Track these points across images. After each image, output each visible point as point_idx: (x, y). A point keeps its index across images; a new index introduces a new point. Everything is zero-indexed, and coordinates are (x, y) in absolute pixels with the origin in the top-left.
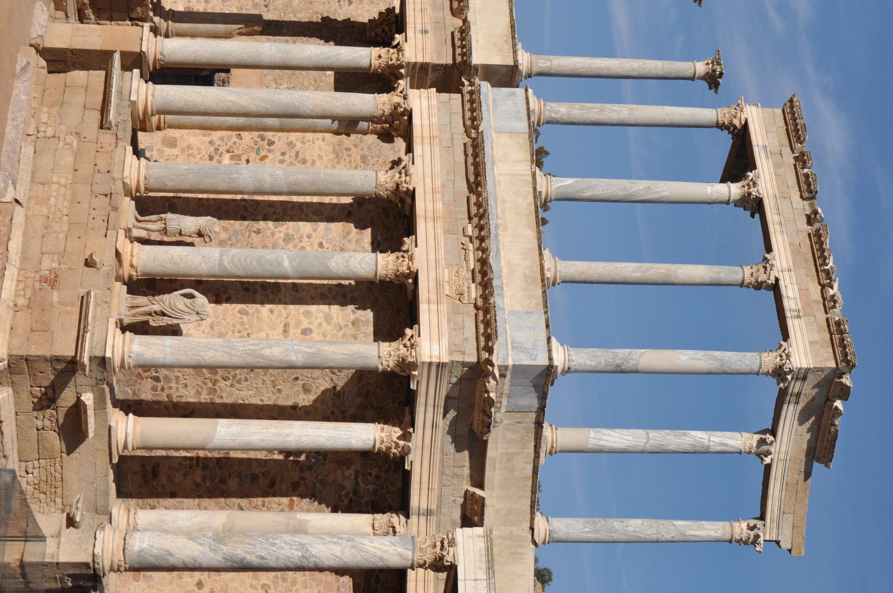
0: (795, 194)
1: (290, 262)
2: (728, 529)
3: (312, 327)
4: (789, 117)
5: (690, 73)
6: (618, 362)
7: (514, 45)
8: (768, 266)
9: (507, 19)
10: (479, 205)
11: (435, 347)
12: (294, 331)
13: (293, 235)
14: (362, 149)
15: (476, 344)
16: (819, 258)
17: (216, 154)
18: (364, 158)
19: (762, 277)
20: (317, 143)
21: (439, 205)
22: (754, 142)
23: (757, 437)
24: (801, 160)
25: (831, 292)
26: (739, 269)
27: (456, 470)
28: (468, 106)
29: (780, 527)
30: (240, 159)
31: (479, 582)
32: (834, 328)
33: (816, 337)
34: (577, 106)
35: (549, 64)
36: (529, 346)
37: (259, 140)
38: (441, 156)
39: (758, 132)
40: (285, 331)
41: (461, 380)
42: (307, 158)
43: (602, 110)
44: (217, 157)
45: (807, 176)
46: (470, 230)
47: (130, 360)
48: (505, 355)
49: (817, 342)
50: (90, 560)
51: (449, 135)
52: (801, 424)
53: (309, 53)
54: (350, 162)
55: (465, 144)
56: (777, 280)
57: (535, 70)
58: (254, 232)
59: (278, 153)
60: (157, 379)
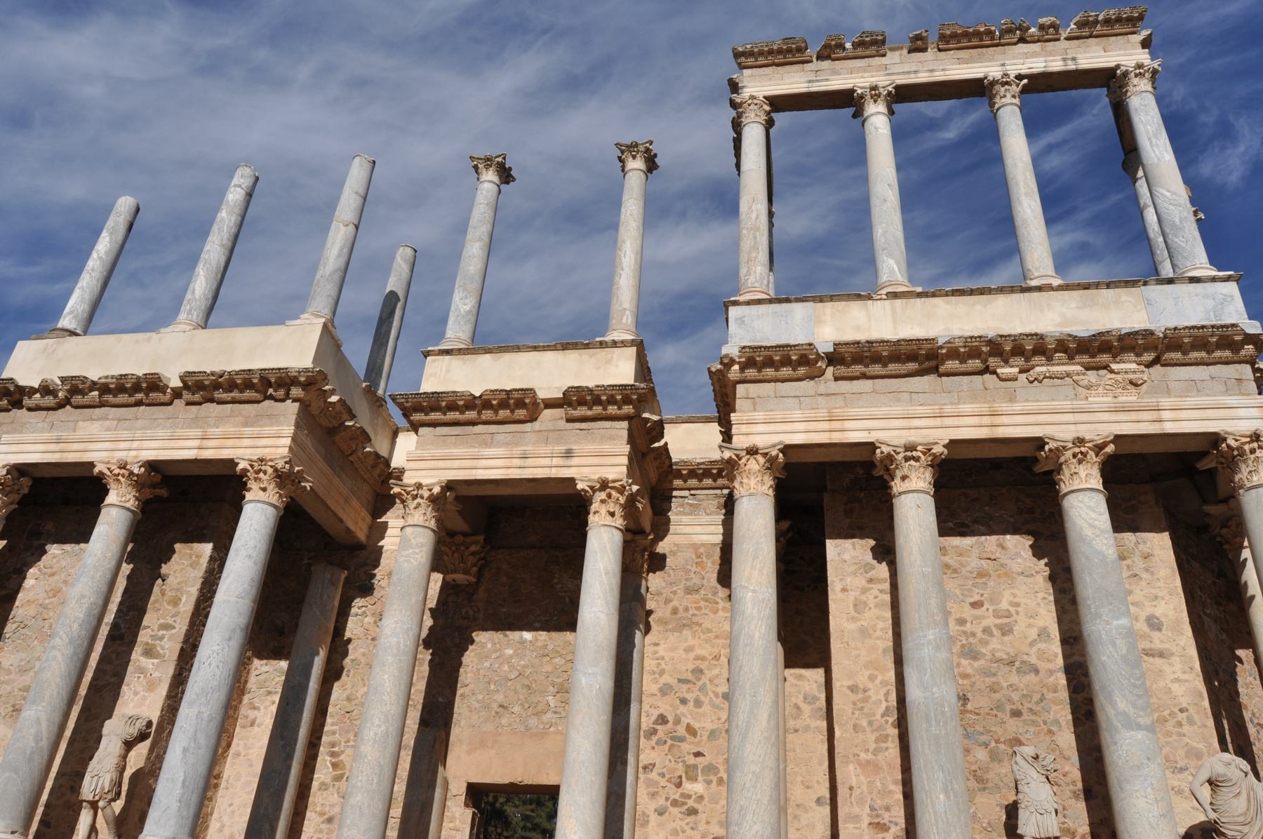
3: (1143, 615)
4: (761, 61)
7: (602, 345)
9: (549, 356)
10: (974, 353)
11: (1242, 412)
12: (1158, 641)
13: (963, 646)
14: (674, 593)
16: (981, 40)
17: (684, 804)
18: (690, 591)
20: (661, 653)
21: (966, 408)
30: (695, 767)
32: (1086, 31)
35: (628, 312)
37: (655, 738)
40: (1161, 654)
42: (691, 667)
44: (691, 803)
45: (856, 45)
51: (820, 398)
53: (603, 616)
54: (698, 609)
55: (836, 379)
58: (964, 705)
59: (682, 709)
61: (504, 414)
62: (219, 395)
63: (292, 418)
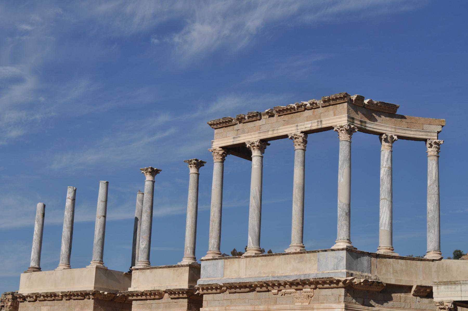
0: (258, 123)
2: (432, 158)
4: (219, 126)
5: (195, 176)
6: (344, 214)
7: (179, 266)
8: (295, 137)
10: (262, 286)
15: (335, 289)
16: (291, 111)
19: (301, 140)
22: (231, 143)
23: (383, 143)
24: (241, 120)
25: (308, 105)
26: (296, 152)
27: (402, 300)
28: (210, 291)
29: (431, 131)
31: (462, 289)
33: (332, 112)
34: (211, 234)
35: (189, 248)
36: (336, 260)
38: (235, 306)
39: (226, 141)
41: (354, 297)
43: (213, 221)
45: (249, 117)
46: (275, 291)
48: (341, 274)
49: (334, 112)
51: (224, 301)
52: (375, 120)
55: (230, 293)
56: (302, 132)
57: (192, 256)
61: (153, 297)
62: (72, 297)
63: (92, 305)
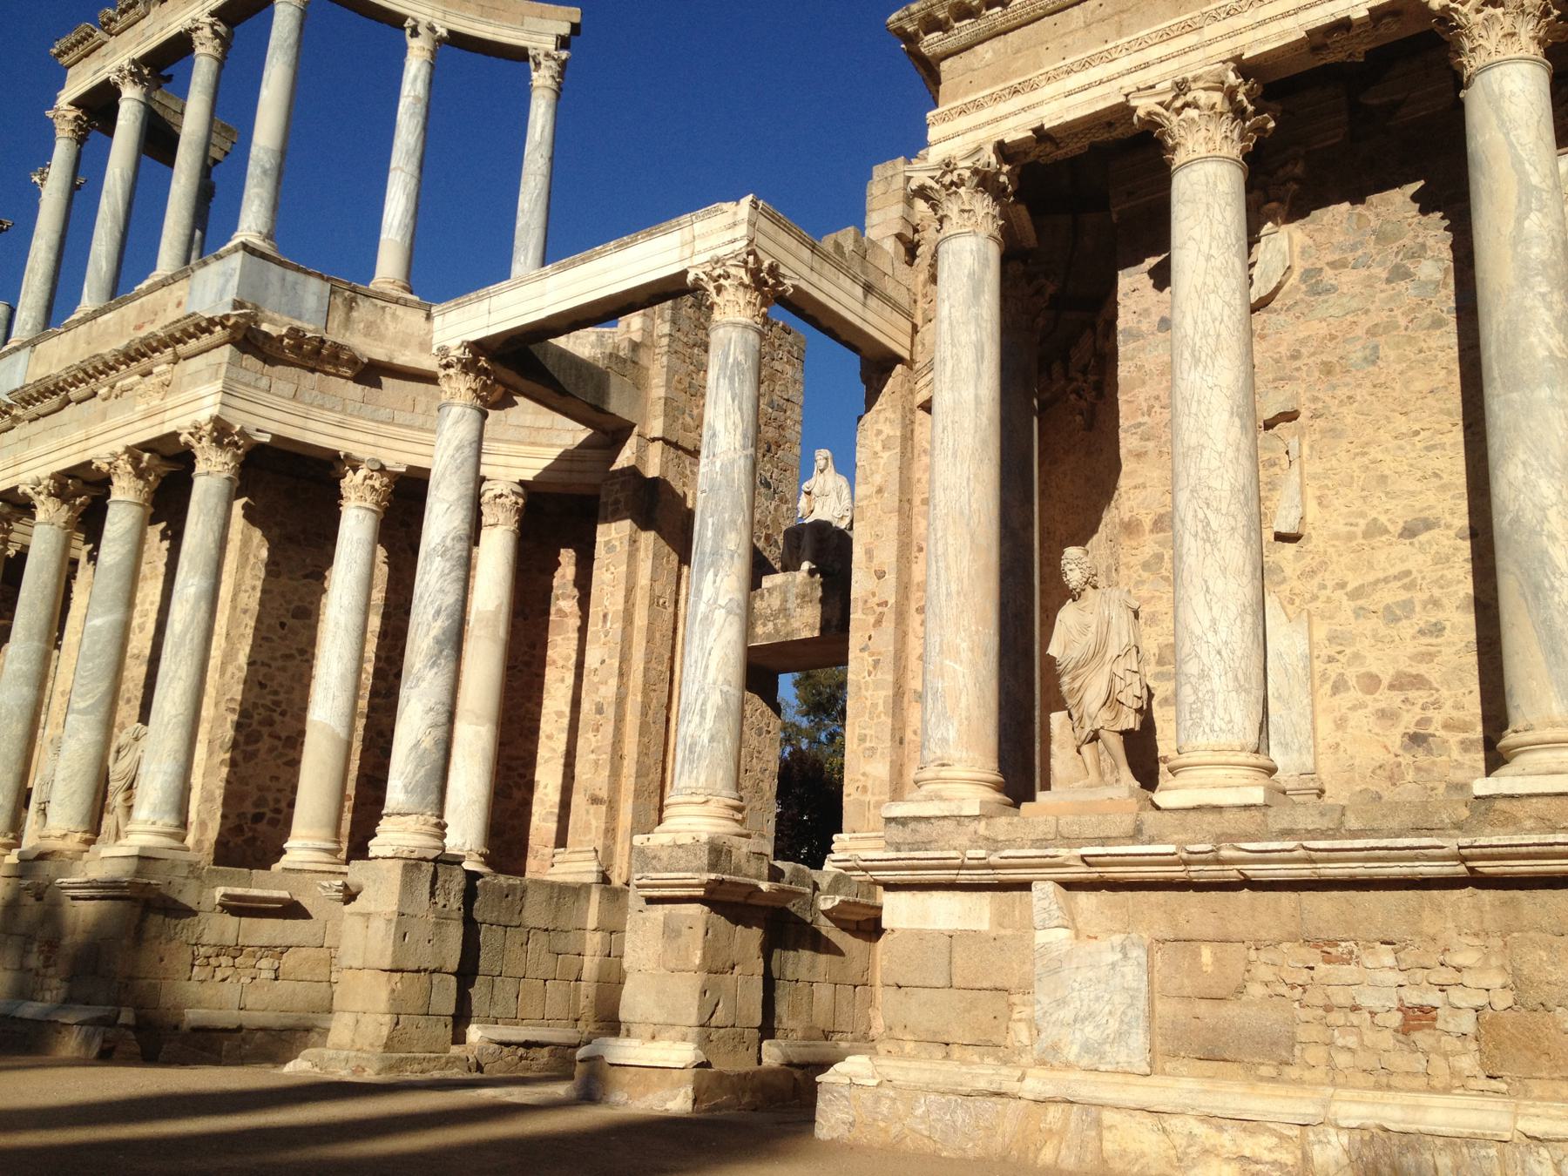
1: (97, 616)
19: (207, 32)
47: (160, 823)
50: (402, 862)
60: (258, 818)
